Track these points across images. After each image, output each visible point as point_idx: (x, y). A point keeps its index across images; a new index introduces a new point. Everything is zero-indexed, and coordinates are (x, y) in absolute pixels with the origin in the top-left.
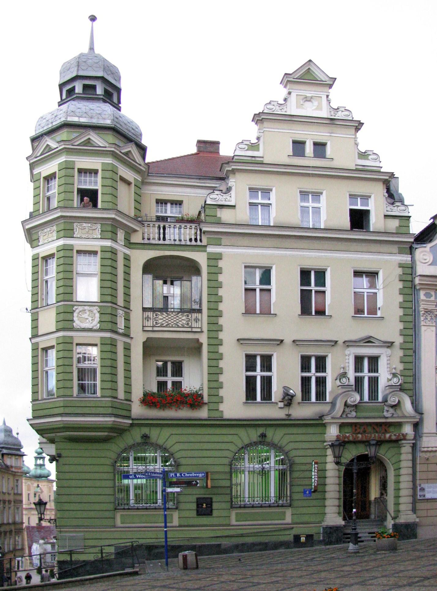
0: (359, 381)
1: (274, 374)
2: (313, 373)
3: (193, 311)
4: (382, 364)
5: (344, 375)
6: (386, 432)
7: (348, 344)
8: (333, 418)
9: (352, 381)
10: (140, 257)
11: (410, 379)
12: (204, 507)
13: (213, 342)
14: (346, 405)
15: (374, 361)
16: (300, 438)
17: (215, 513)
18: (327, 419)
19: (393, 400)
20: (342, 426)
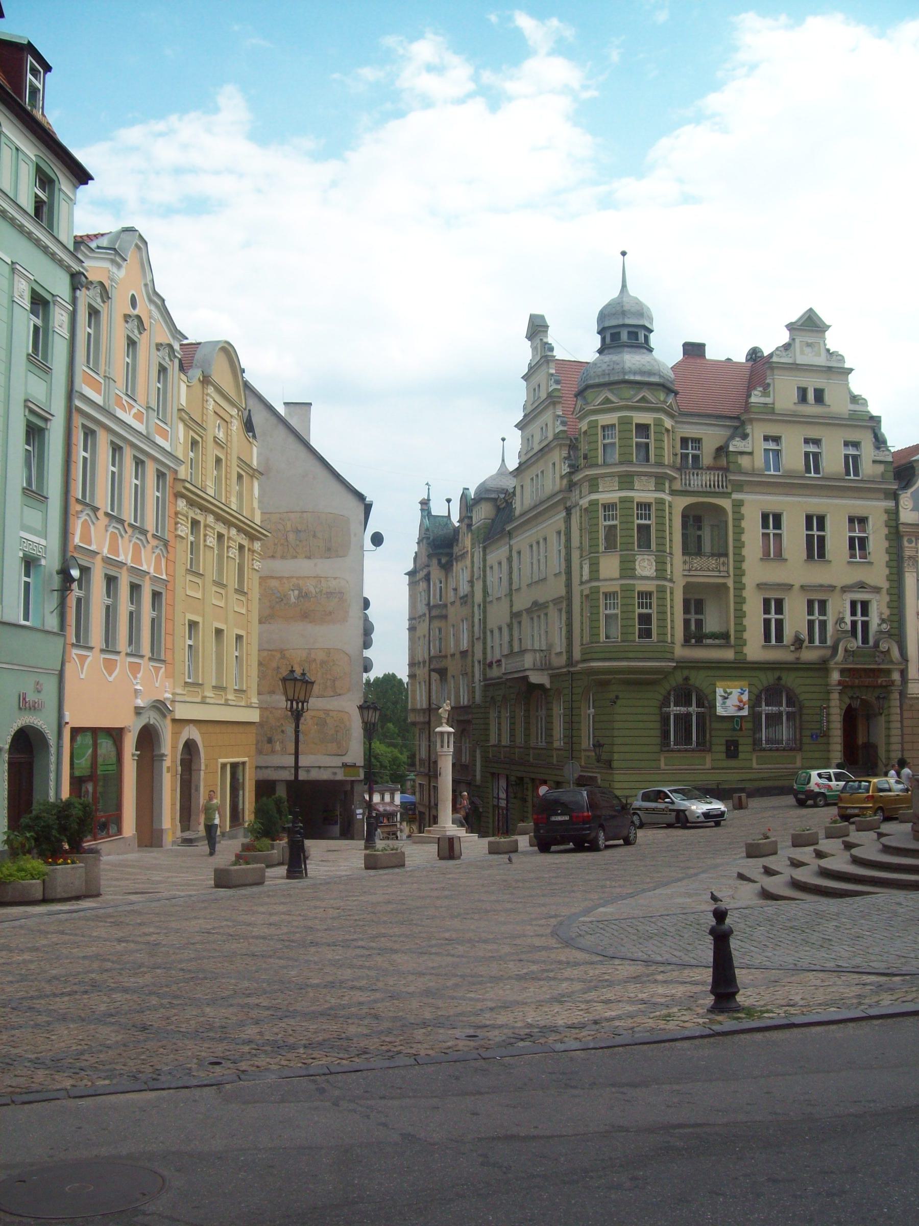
0: (854, 624)
1: (787, 616)
2: (816, 616)
3: (720, 555)
4: (874, 610)
5: (841, 620)
6: (878, 677)
7: (845, 589)
8: (836, 663)
9: (849, 627)
10: (681, 503)
11: (895, 625)
12: (732, 750)
13: (738, 586)
14: (846, 650)
15: (865, 605)
16: (808, 681)
17: (741, 756)
18: (832, 664)
19: (884, 646)
20: (843, 671)
